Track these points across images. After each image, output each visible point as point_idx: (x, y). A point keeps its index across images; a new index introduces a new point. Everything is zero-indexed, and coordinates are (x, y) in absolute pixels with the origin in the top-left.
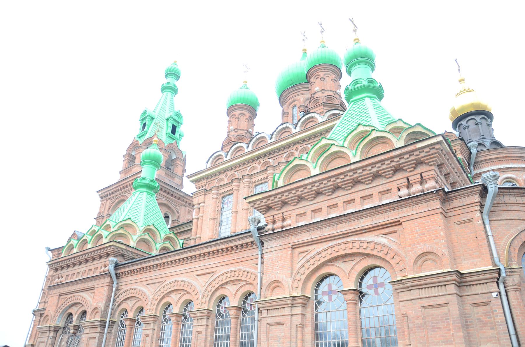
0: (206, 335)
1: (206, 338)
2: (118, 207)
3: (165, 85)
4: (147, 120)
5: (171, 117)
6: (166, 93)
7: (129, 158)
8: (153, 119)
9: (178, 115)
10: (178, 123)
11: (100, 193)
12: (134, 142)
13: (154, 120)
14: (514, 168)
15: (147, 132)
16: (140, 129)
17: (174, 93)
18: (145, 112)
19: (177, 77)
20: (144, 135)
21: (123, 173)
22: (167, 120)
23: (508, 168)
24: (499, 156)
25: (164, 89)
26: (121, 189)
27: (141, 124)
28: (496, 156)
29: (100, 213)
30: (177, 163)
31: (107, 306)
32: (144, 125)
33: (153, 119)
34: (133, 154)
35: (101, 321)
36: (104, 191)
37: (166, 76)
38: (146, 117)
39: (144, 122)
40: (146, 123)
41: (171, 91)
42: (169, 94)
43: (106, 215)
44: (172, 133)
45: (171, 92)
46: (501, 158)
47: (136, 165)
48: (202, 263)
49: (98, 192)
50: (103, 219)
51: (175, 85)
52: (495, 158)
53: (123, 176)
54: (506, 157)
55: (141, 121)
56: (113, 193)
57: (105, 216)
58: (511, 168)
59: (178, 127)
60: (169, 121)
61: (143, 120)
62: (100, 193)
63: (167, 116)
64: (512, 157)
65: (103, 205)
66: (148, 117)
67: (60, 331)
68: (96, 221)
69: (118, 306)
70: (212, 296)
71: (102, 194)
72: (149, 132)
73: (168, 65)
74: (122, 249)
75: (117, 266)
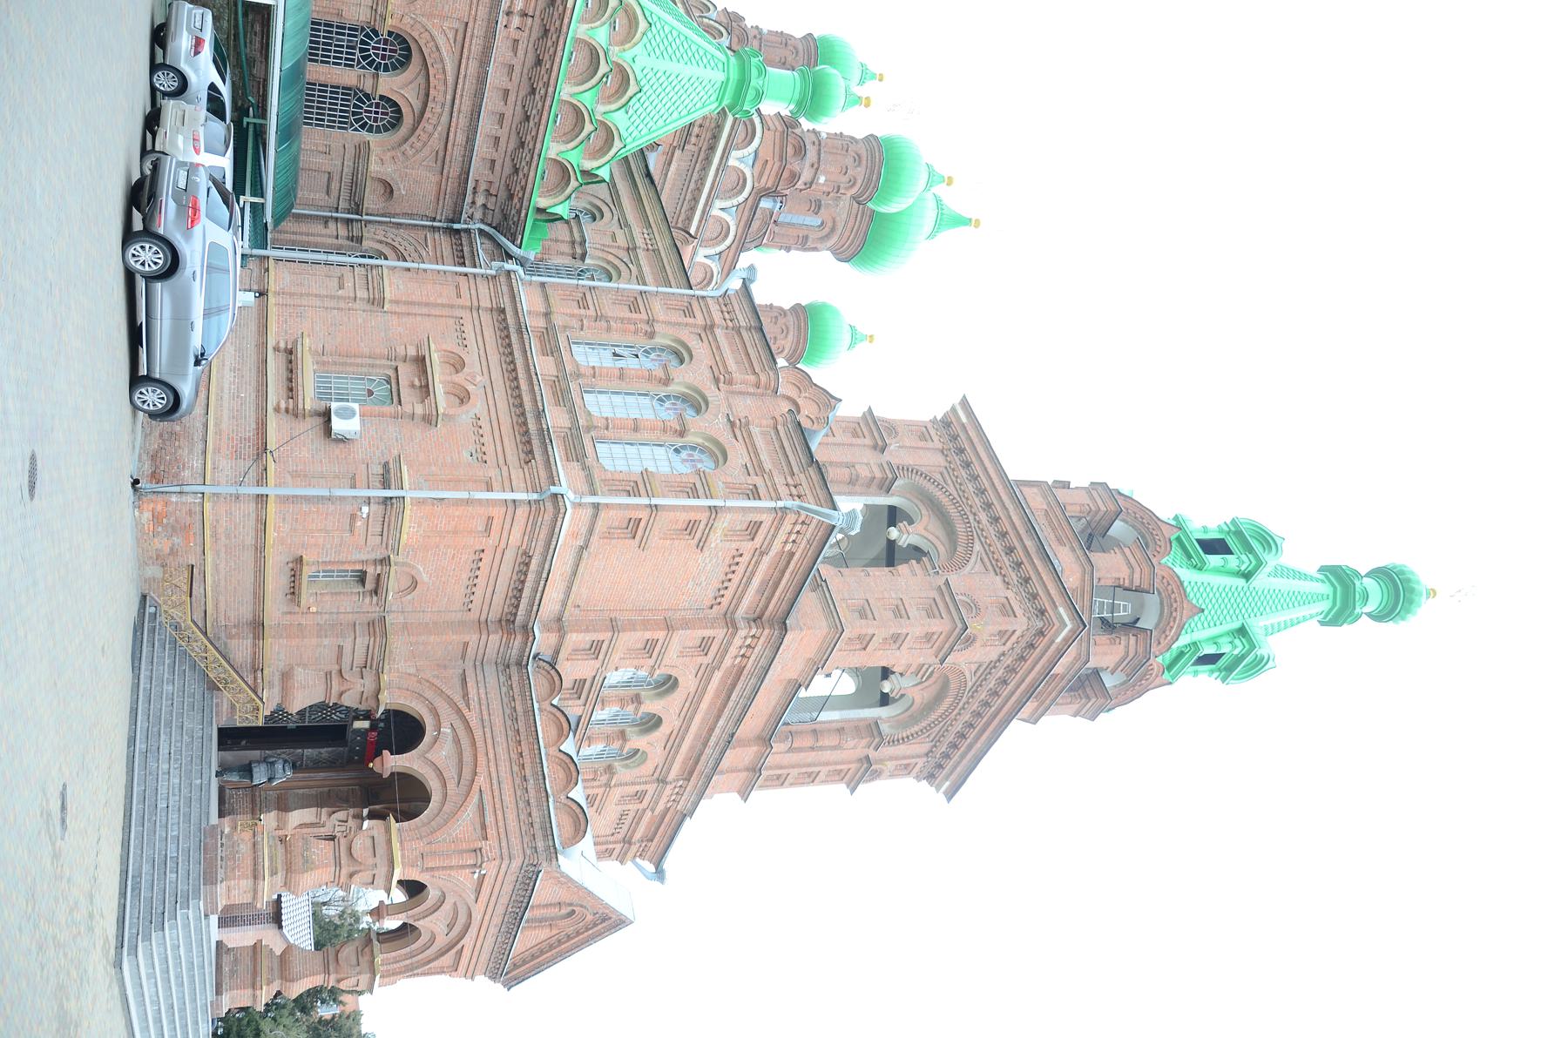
2: (924, 512)
3: (1357, 583)
4: (1244, 557)
5: (1253, 647)
6: (1326, 589)
7: (1101, 513)
8: (1247, 576)
9: (1259, 664)
10: (1229, 669)
11: (964, 419)
12: (1159, 522)
13: (1242, 582)
15: (1200, 569)
16: (1205, 530)
17: (1330, 616)
18: (1268, 541)
19: (1384, 615)
20: (1189, 557)
21: (1045, 497)
22: (1242, 632)
25: (1340, 577)
26: (996, 520)
27: (1221, 531)
29: (892, 428)
30: (1089, 699)
32: (1214, 547)
33: (1247, 576)
34: (1118, 528)
36: (972, 434)
37: (1382, 574)
38: (1250, 549)
39: (1232, 543)
40: (1229, 551)
41: (1336, 608)
42: (1325, 605)
43: (889, 464)
45: (1331, 610)
47: (1088, 568)
49: (964, 403)
50: (875, 447)
51: (1358, 617)
53: (1036, 501)
55: (1233, 529)
56: (975, 478)
57: (886, 457)
59: (1212, 672)
60: (1237, 642)
61: (1239, 534)
62: (964, 419)
63: (1256, 626)
65: (922, 437)
66: (1254, 562)
68: (860, 415)
71: (1053, 642)
73: (1423, 573)
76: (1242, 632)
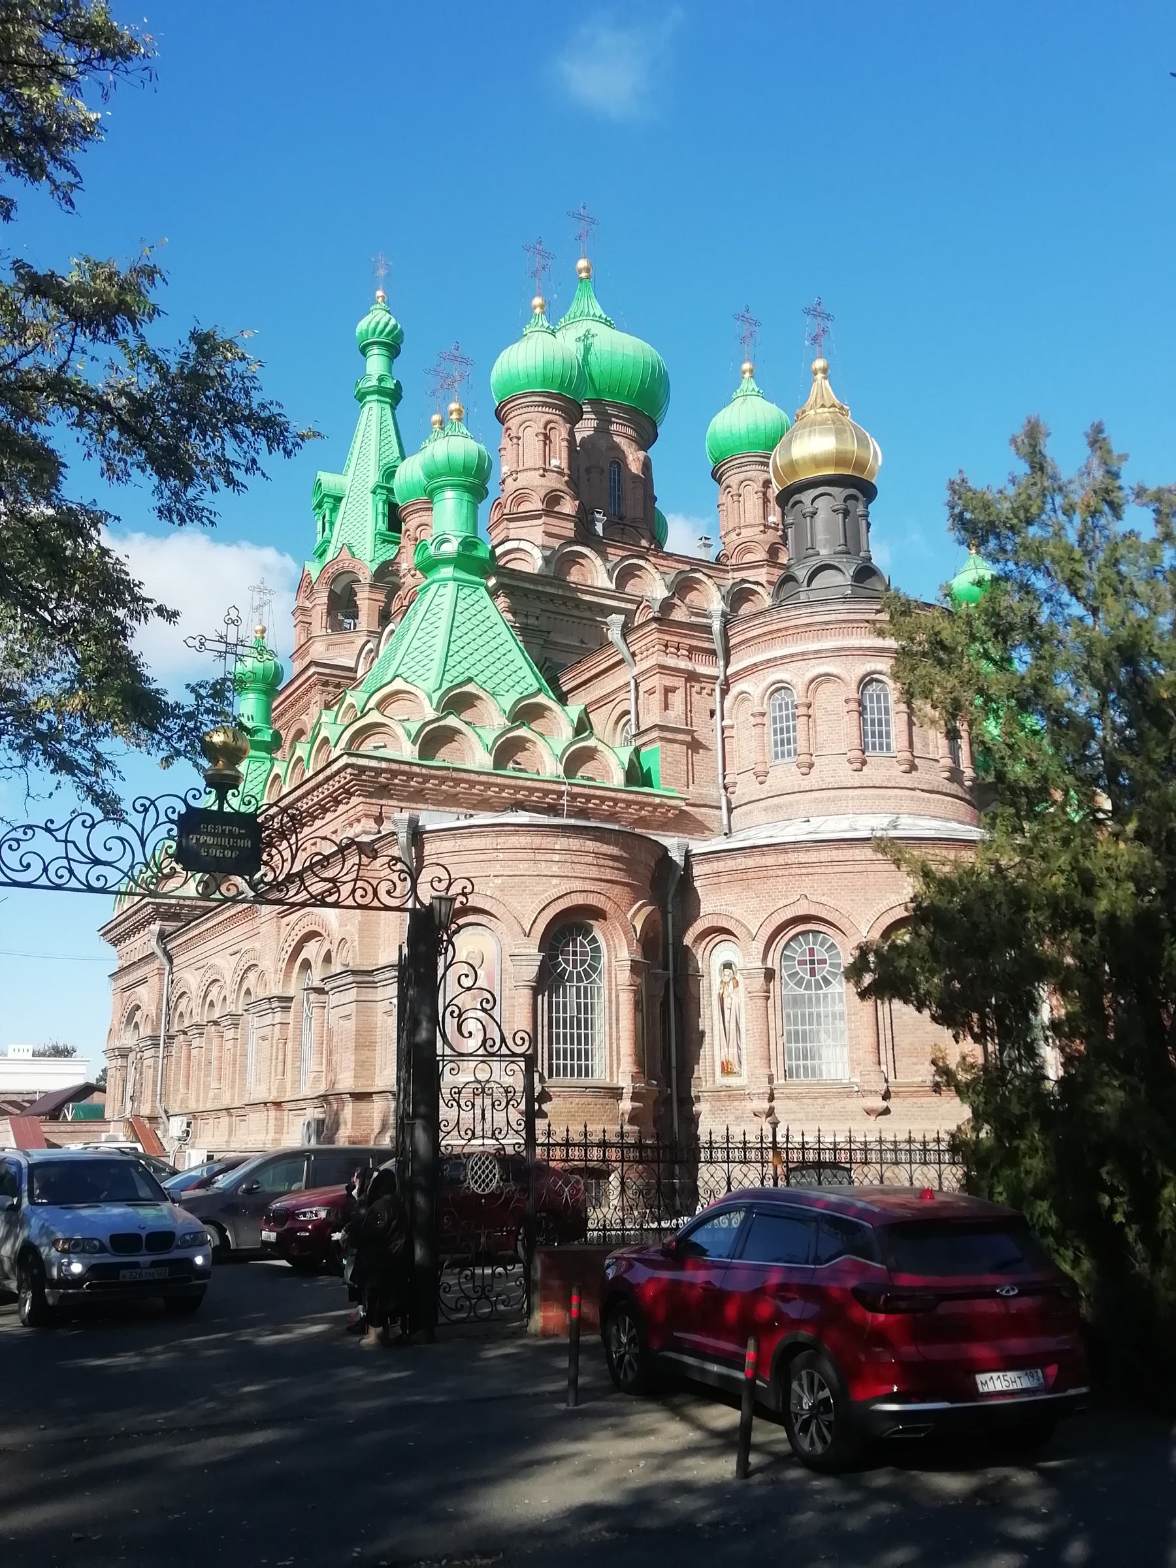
0: (235, 1055)
1: (235, 1061)
8: (338, 499)
14: (792, 655)
22: (374, 492)
23: (781, 658)
24: (766, 629)
28: (760, 631)
31: (159, 1009)
35: (152, 1038)
44: (390, 529)
46: (770, 633)
48: (232, 934)
52: (759, 636)
54: (780, 630)
58: (786, 656)
64: (791, 627)
67: (132, 1056)
69: (175, 1009)
70: (239, 990)
72: (333, 541)
74: (170, 906)
75: (162, 936)
76: (374, 492)
